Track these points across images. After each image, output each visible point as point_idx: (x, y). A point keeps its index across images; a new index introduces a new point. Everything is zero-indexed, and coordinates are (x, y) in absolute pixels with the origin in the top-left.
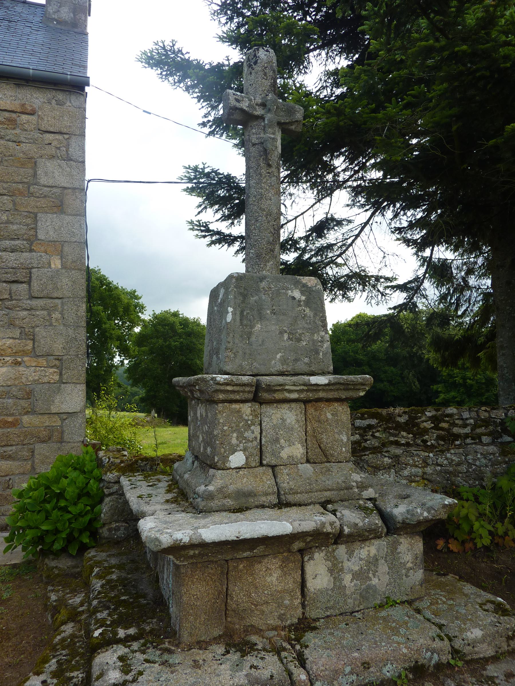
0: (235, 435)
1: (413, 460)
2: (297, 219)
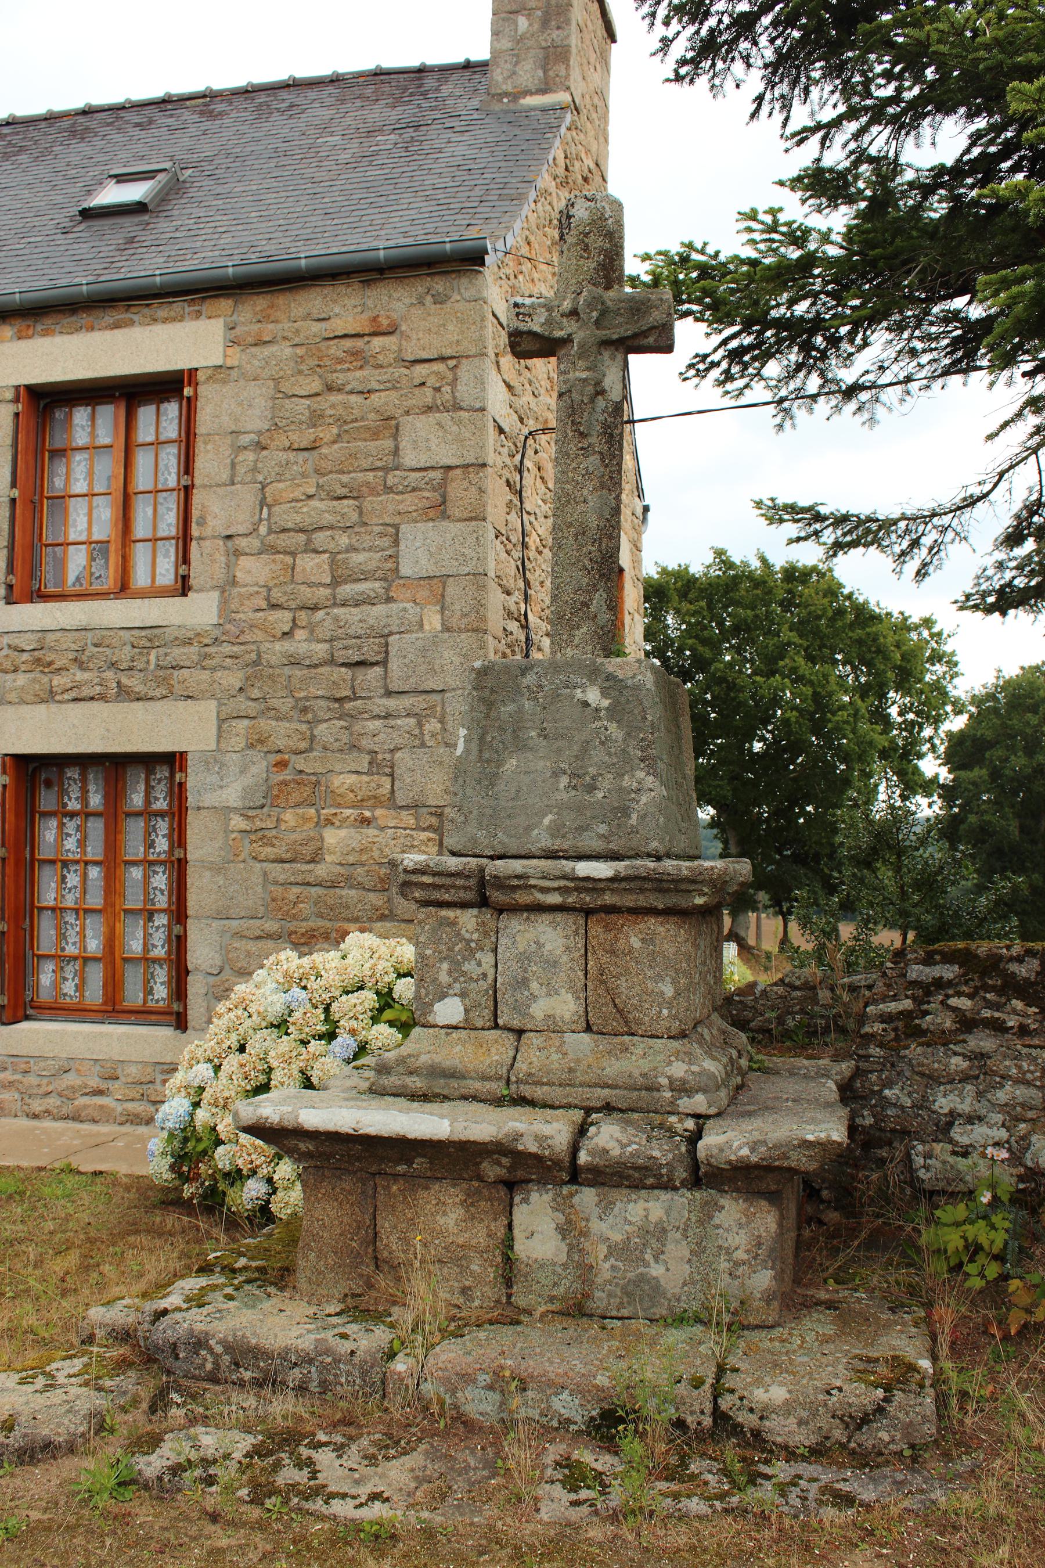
0: (445, 966)
1: (1019, 1067)
2: (1040, 453)
